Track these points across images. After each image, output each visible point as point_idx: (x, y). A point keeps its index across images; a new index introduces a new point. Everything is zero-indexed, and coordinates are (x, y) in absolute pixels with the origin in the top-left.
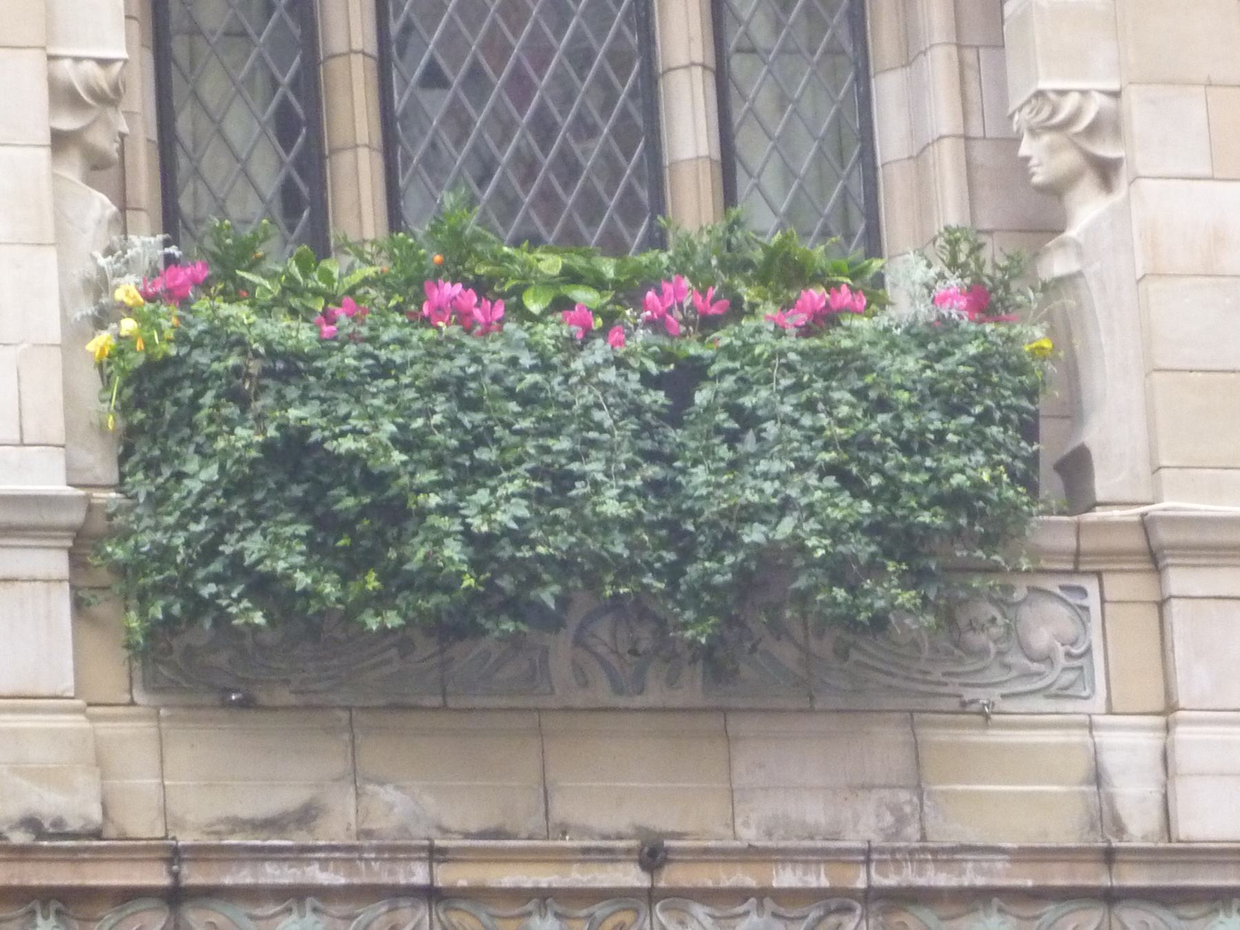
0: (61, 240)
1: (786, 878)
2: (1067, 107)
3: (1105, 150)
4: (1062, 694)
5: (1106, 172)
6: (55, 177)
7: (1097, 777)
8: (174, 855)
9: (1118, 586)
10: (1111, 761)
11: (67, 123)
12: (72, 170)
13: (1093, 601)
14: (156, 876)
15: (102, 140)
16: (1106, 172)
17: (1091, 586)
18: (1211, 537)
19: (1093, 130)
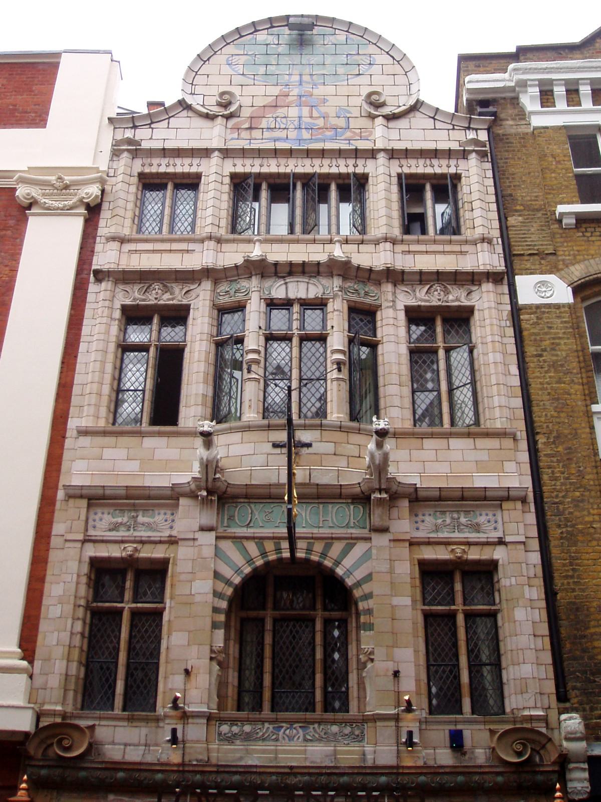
0: (210, 673)
1: (311, 771)
2: (366, 650)
3: (372, 657)
4: (360, 741)
5: (372, 660)
6: (210, 664)
7: (364, 755)
8: (218, 766)
9: (370, 724)
10: (366, 752)
11: (213, 656)
12: (214, 663)
13: (366, 727)
14: (215, 769)
15: (219, 658)
16: (372, 660)
17: (365, 725)
18: (385, 717)
19: (370, 654)
